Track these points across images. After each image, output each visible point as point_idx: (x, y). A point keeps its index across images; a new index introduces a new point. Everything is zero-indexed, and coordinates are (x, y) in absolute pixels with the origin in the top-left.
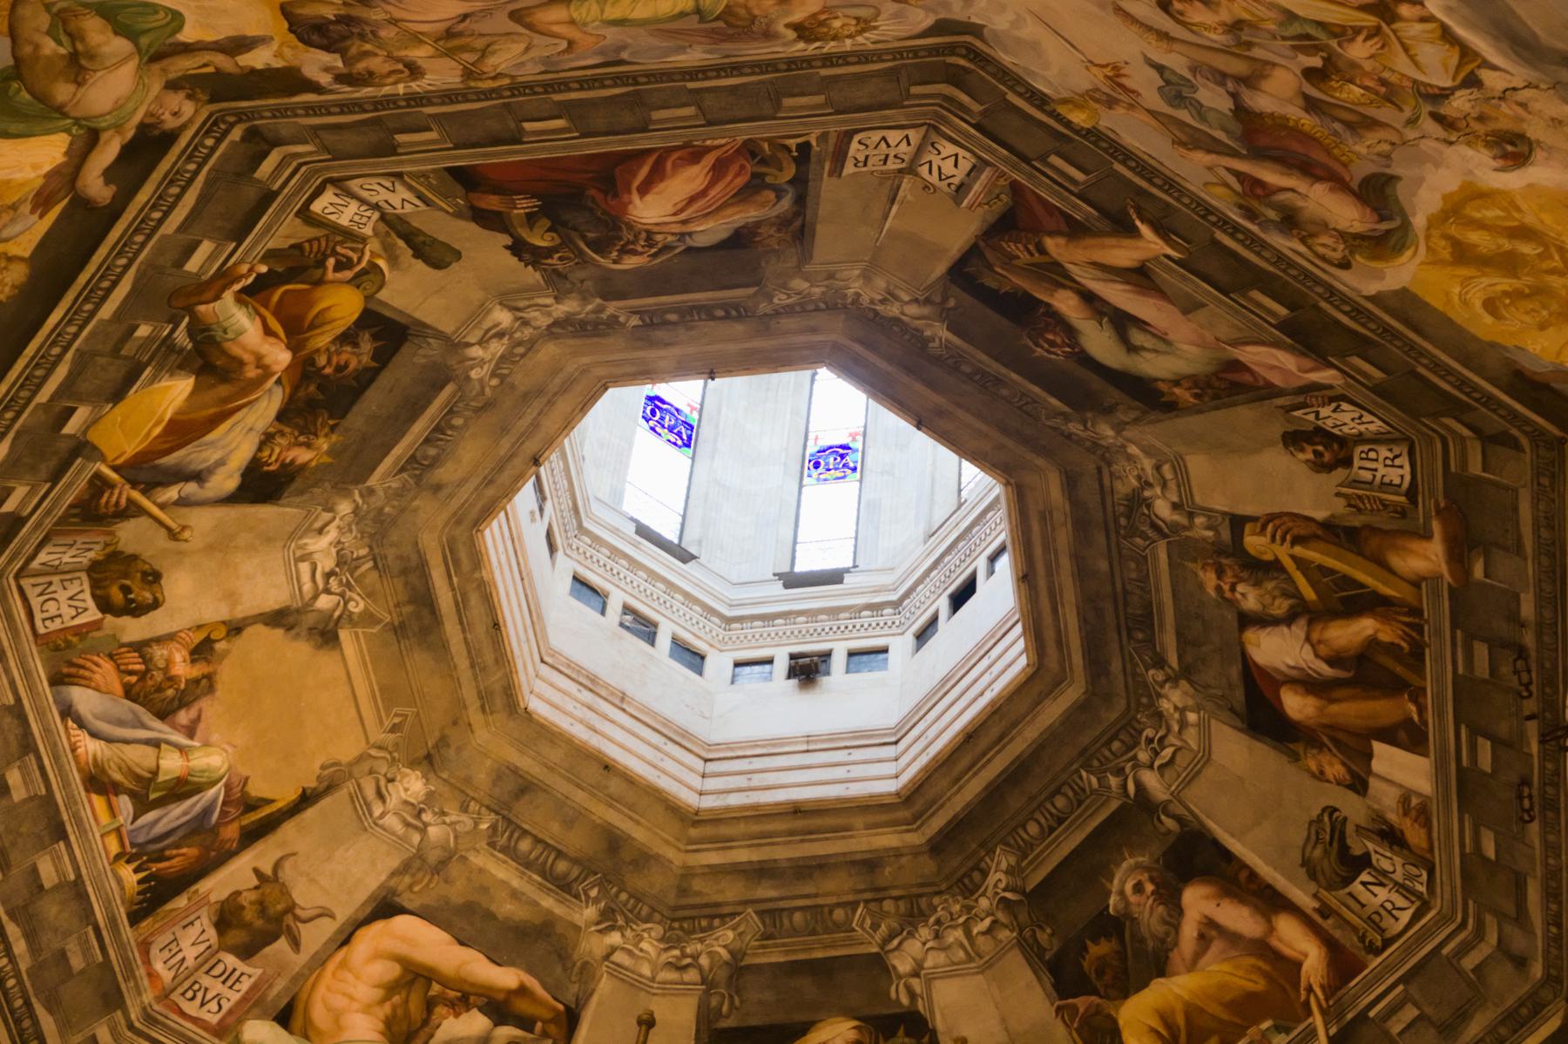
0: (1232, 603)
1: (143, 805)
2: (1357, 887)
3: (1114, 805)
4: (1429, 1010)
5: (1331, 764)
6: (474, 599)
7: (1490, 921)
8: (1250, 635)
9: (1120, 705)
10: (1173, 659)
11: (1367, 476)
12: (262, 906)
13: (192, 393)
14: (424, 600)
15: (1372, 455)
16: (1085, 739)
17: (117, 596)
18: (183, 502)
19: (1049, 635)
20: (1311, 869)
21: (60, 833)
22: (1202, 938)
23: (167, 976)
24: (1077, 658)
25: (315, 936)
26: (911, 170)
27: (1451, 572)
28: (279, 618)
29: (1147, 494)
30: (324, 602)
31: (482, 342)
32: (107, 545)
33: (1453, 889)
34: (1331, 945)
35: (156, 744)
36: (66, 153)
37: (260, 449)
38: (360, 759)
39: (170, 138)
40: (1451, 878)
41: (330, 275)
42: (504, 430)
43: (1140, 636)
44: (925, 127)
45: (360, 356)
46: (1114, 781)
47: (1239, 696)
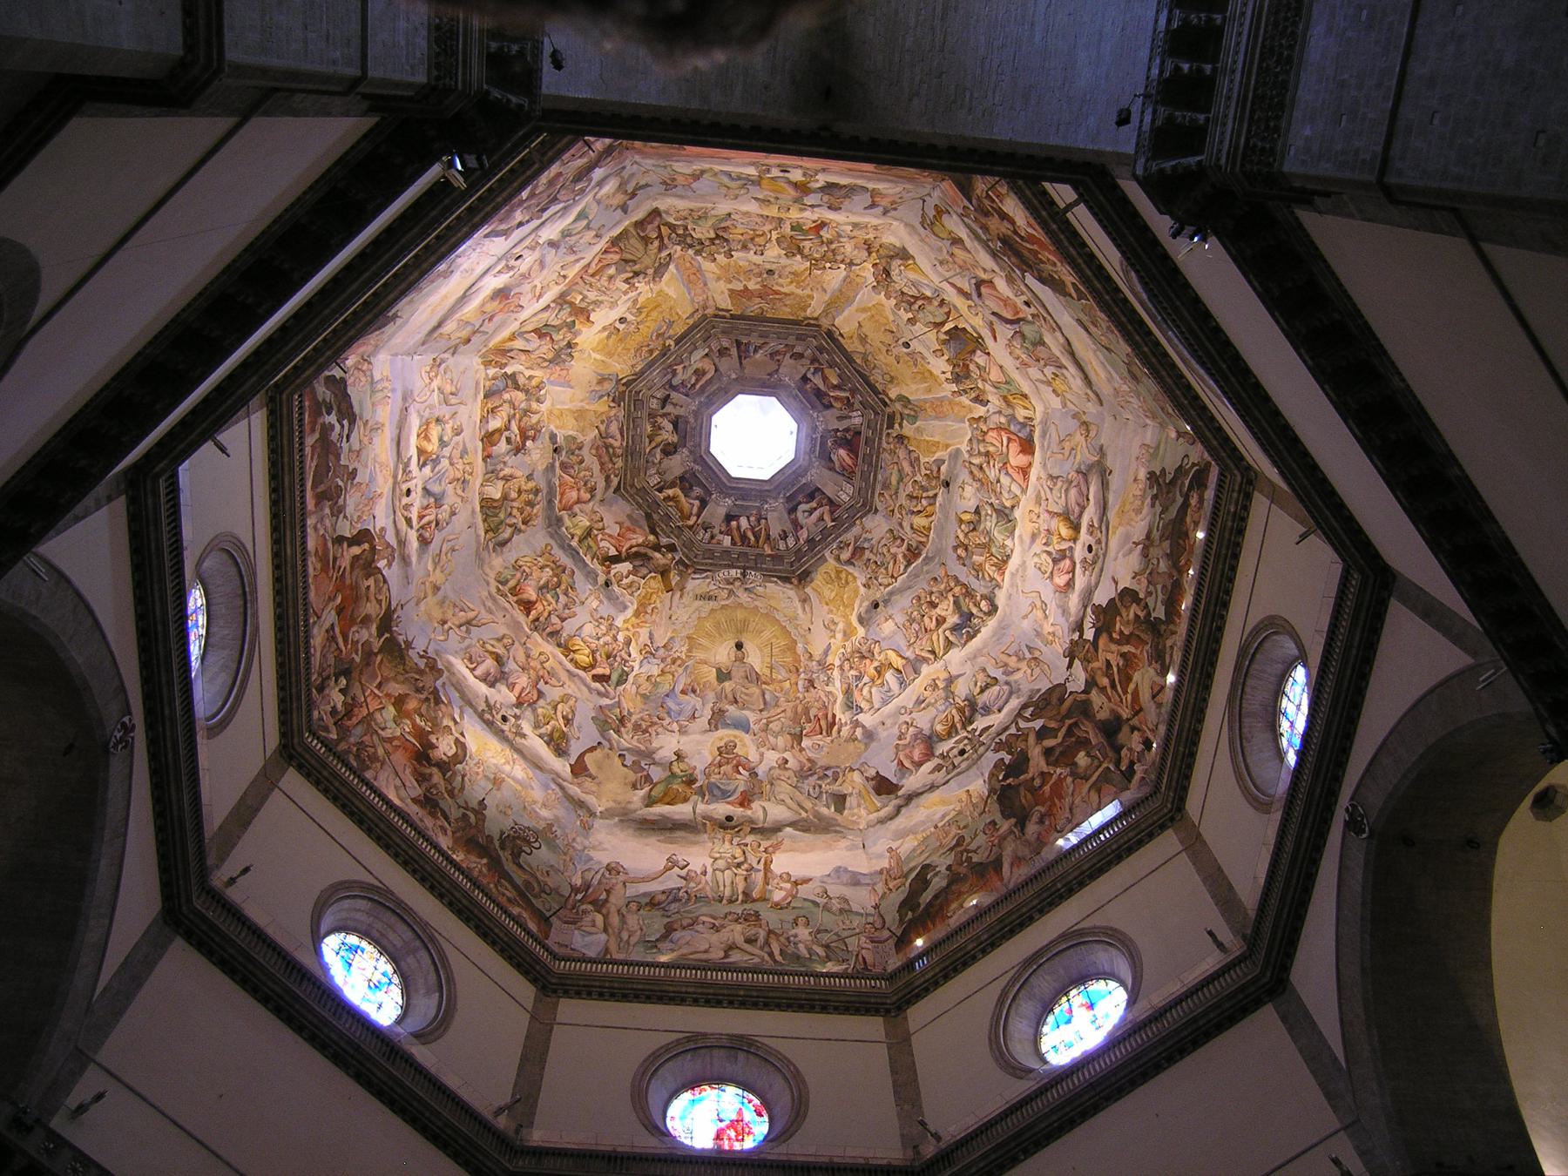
25: (717, 360)
45: (825, 401)
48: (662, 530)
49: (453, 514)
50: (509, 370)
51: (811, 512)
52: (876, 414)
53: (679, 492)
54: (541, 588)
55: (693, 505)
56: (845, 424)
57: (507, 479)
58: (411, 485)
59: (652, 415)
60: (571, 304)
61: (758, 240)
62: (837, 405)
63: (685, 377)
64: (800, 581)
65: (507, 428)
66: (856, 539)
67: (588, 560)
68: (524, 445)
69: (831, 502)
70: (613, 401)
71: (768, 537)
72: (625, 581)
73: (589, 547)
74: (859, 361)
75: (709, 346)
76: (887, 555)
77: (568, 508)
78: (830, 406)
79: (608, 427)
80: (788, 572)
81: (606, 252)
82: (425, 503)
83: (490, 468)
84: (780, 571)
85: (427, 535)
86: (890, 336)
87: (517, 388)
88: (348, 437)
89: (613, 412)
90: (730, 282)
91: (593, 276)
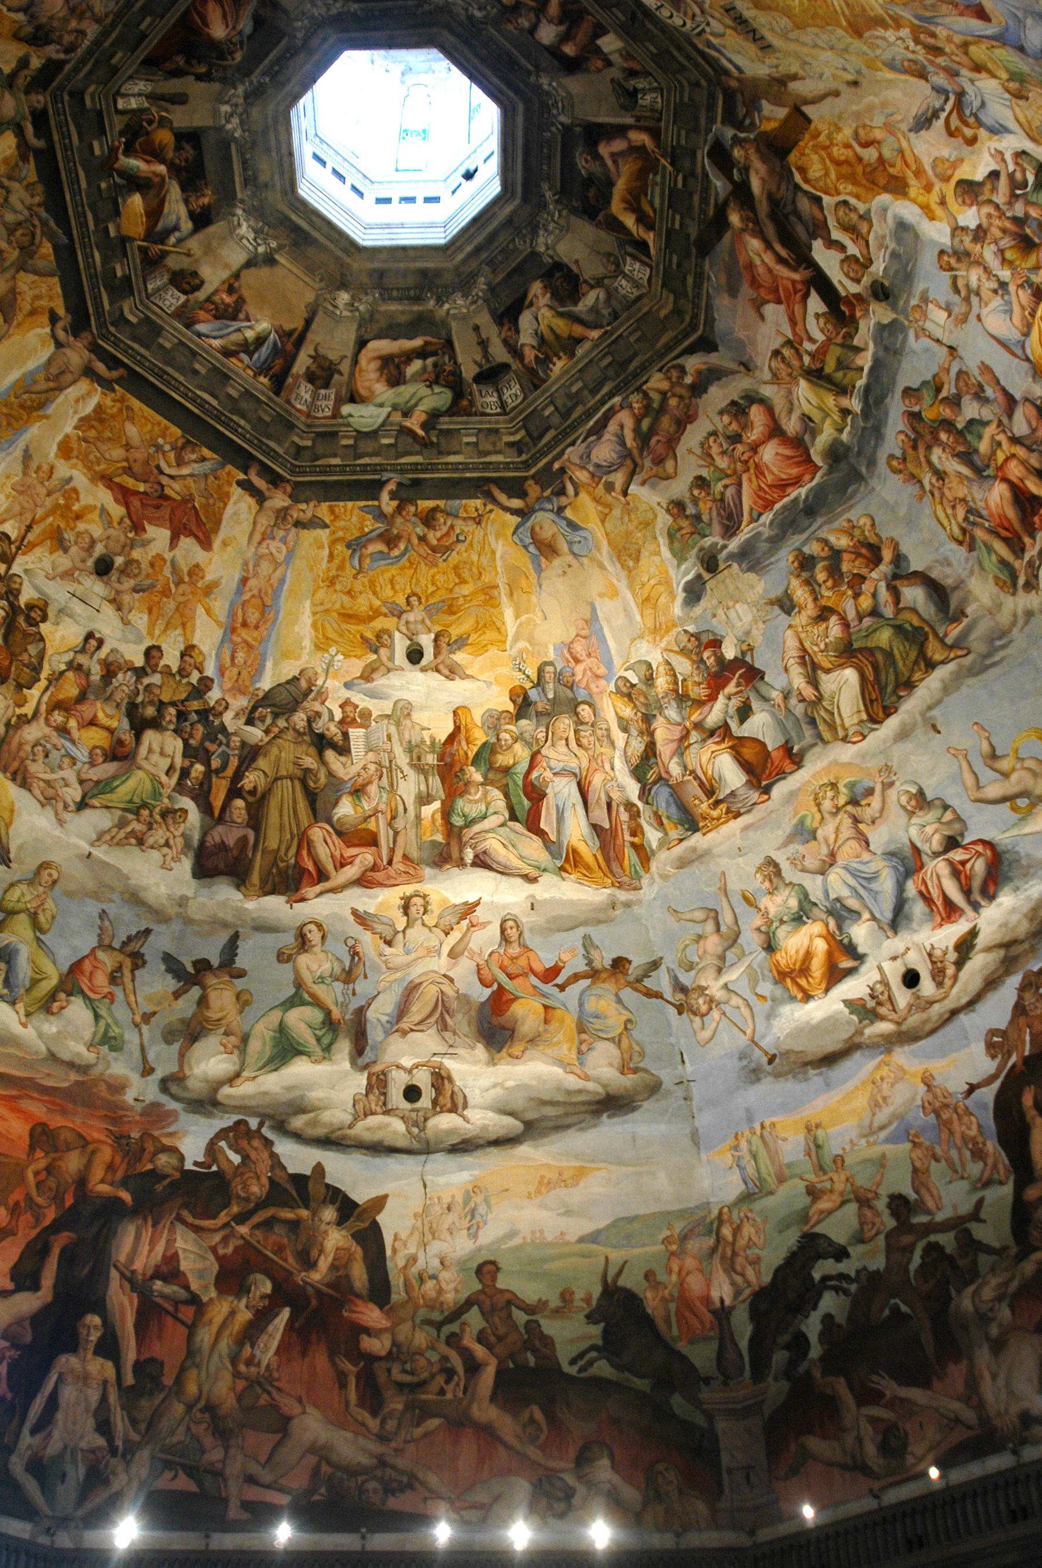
0: (522, 30)
1: (250, 354)
12: (320, 367)
14: (296, 229)
18: (180, 241)
20: (625, 108)
21: (226, 378)
22: (615, 162)
23: (304, 408)
24: (512, 94)
28: (249, 264)
30: (261, 250)
31: (228, 121)
34: (648, 130)
35: (239, 330)
38: (317, 298)
39: (44, 112)
42: (268, 150)
48: (704, 200)
49: (921, 801)
50: (633, 789)
52: (78, 96)
53: (616, 206)
54: (978, 471)
55: (613, 156)
57: (812, 670)
58: (894, 972)
59: (533, 380)
60: (447, 813)
61: (70, 689)
62: (164, 137)
63: (423, 390)
65: (723, 731)
67: (865, 360)
68: (738, 662)
70: (562, 492)
72: (853, 249)
73: (841, 365)
74: (47, 249)
75: (336, 414)
77: (799, 445)
79: (610, 469)
81: (322, 876)
82: (918, 908)
83: (808, 732)
85: (979, 867)
87: (650, 751)
88: (841, 1254)
89: (582, 476)
90: (196, 571)
91: (372, 840)
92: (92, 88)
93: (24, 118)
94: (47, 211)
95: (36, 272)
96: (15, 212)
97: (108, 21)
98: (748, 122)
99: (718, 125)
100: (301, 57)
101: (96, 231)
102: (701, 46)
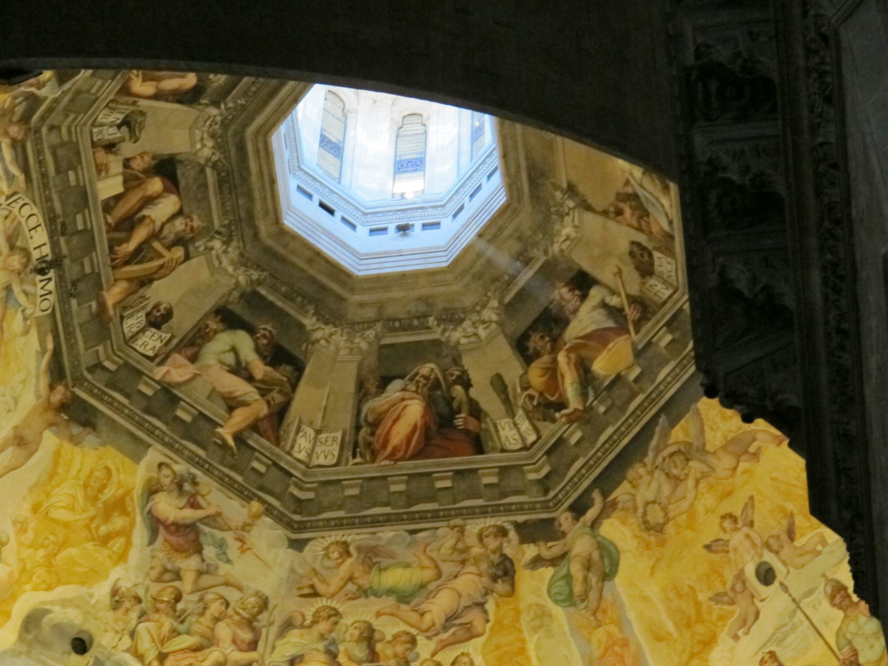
2: (121, 117)
3: (229, 98)
4: (86, 95)
5: (139, 165)
6: (513, 169)
7: (65, 137)
8: (177, 207)
9: (230, 132)
10: (208, 171)
11: (139, 314)
13: (592, 361)
14: (532, 181)
15: (138, 325)
16: (245, 114)
17: (645, 254)
18: (613, 292)
19: (262, 154)
20: (142, 113)
24: (250, 147)
26: (318, 432)
27: (102, 296)
28: (589, 208)
29: (224, 247)
30: (571, 204)
31: (491, 321)
32: (644, 284)
33: (83, 142)
35: (641, 185)
36: (601, 524)
37: (579, 307)
40: (84, 145)
41: (536, 395)
43: (223, 174)
44: (311, 465)
46: (231, 105)
47: (179, 172)
51: (239, 369)
52: (545, 484)
56: (489, 402)
62: (536, 375)
64: (63, 407)
66: (213, 520)
69: (280, 414)
71: (145, 281)
74: (678, 434)
76: (206, 620)
78: (527, 356)
80: (75, 367)
84: (72, 347)
86: (778, 527)
92: (532, 476)
93: (584, 525)
94: (645, 454)
95: (702, 432)
96: (660, 486)
97: (458, 521)
98: (18, 101)
99: (51, 97)
100: (390, 311)
101: (642, 390)
102: (21, 177)
